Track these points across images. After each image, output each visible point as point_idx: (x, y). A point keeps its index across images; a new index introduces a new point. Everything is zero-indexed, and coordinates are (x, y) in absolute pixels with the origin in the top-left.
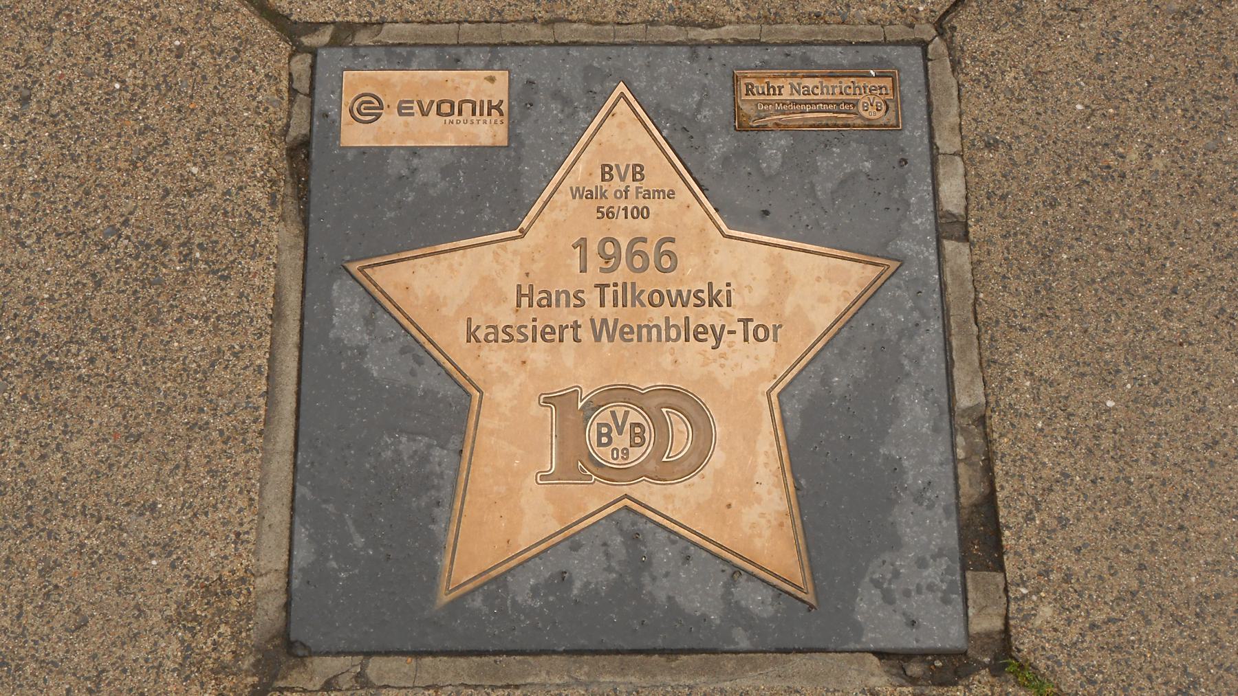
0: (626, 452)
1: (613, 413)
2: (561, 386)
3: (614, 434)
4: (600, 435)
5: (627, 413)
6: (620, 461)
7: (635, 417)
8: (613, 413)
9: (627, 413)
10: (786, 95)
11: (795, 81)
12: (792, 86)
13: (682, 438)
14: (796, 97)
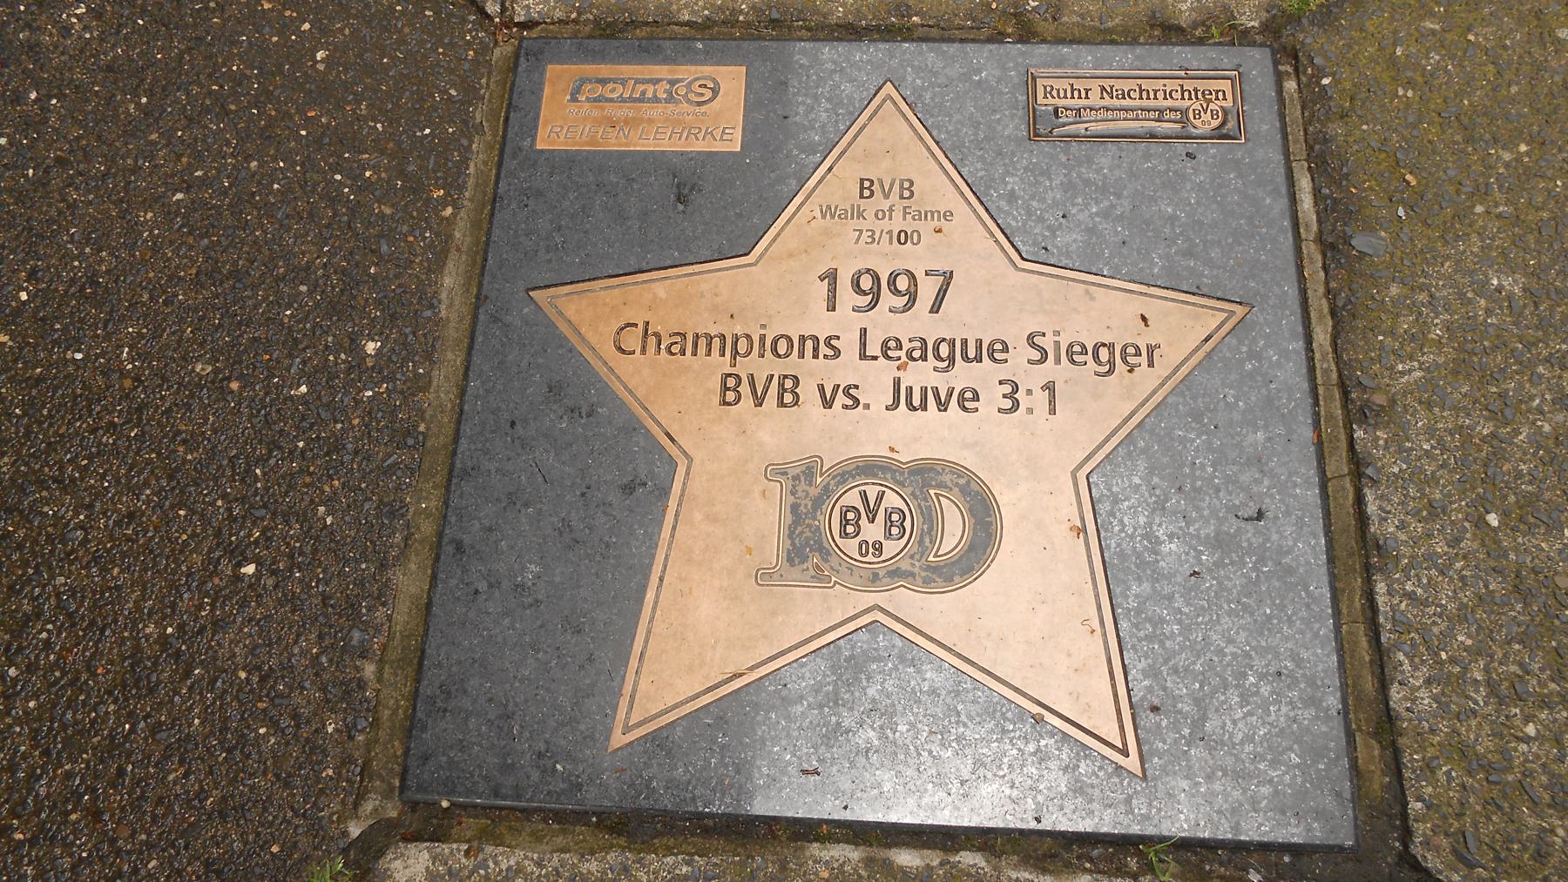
0: (878, 548)
1: (864, 495)
2: (794, 454)
3: (864, 521)
4: (845, 522)
5: (881, 496)
6: (870, 558)
7: (892, 500)
8: (864, 495)
9: (881, 496)
10: (1095, 99)
11: (1107, 83)
12: (1103, 89)
13: (954, 530)
14: (1107, 102)
